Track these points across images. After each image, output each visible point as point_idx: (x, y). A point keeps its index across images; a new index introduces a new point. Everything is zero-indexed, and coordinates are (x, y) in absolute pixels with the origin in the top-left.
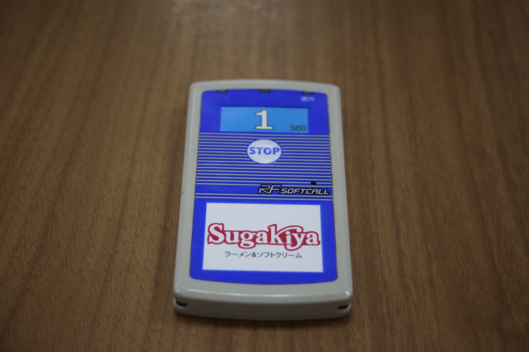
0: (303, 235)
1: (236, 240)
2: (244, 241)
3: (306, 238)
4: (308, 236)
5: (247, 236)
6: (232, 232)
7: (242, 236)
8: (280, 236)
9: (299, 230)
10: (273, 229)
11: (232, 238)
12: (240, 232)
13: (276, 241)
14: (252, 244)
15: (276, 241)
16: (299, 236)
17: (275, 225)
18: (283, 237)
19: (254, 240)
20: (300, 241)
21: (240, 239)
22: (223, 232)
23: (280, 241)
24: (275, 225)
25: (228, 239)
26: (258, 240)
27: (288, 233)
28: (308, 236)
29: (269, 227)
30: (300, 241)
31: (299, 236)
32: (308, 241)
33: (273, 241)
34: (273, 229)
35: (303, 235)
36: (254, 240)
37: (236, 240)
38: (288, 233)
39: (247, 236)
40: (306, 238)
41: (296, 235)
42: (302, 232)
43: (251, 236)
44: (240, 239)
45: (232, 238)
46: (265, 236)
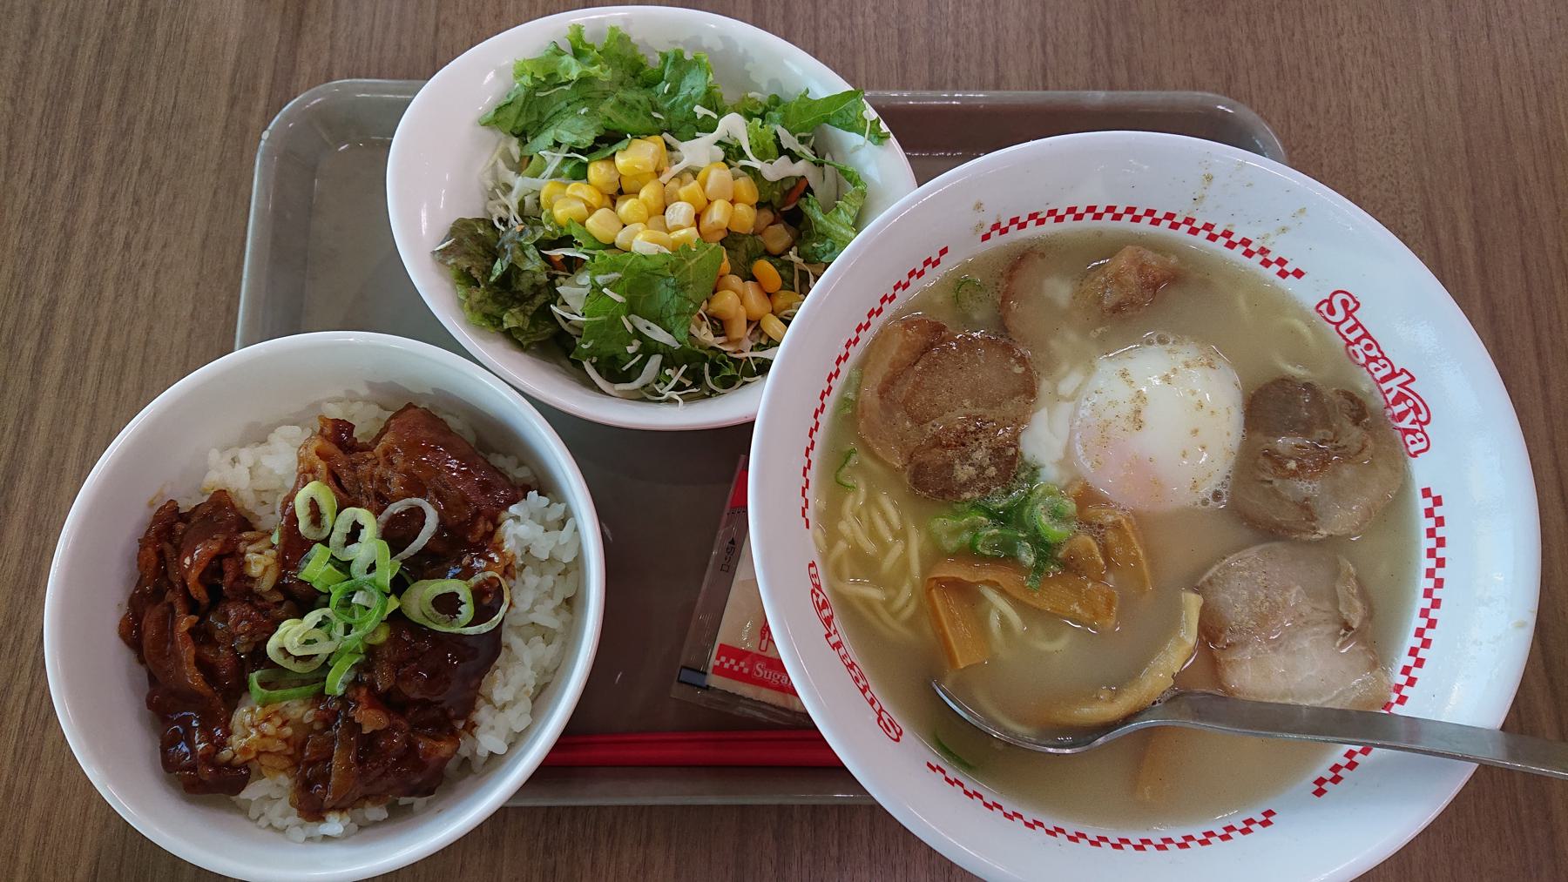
0: (1417, 426)
1: (1351, 337)
2: (1357, 348)
3: (1414, 432)
4: (1420, 435)
5: (1368, 347)
6: (1358, 325)
7: (1365, 341)
8: (1399, 393)
9: (1423, 418)
10: (1405, 378)
11: (1349, 331)
12: (1366, 335)
13: (1390, 391)
14: (1362, 360)
15: (1390, 391)
16: (1413, 422)
17: (1413, 379)
18: (1400, 398)
19: (1370, 359)
20: (1405, 424)
21: (1358, 341)
22: (1349, 314)
23: (1390, 397)
24: (1413, 379)
25: (1343, 328)
26: (1372, 366)
27: (1410, 403)
28: (1420, 435)
29: (1403, 370)
30: (1405, 424)
31: (1413, 422)
32: (1409, 438)
33: (1385, 387)
34: (1405, 378)
35: (1417, 426)
36: (1370, 359)
37: (1351, 337)
38: (1410, 403)
39: (1368, 347)
40: (1414, 432)
41: (1412, 416)
42: (1422, 424)
43: (1373, 353)
44: (1358, 341)
45: (1349, 331)
46: (1388, 371)
